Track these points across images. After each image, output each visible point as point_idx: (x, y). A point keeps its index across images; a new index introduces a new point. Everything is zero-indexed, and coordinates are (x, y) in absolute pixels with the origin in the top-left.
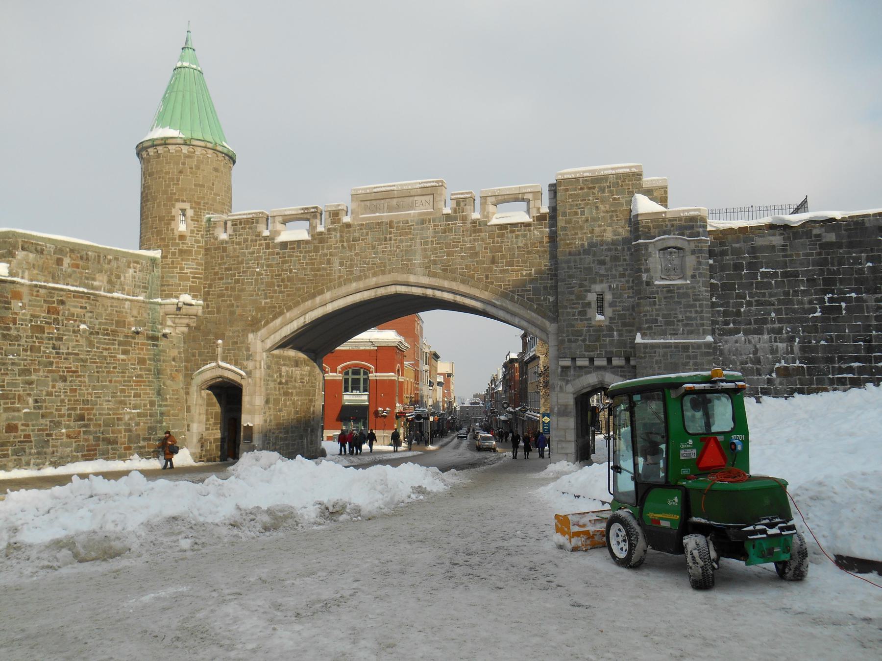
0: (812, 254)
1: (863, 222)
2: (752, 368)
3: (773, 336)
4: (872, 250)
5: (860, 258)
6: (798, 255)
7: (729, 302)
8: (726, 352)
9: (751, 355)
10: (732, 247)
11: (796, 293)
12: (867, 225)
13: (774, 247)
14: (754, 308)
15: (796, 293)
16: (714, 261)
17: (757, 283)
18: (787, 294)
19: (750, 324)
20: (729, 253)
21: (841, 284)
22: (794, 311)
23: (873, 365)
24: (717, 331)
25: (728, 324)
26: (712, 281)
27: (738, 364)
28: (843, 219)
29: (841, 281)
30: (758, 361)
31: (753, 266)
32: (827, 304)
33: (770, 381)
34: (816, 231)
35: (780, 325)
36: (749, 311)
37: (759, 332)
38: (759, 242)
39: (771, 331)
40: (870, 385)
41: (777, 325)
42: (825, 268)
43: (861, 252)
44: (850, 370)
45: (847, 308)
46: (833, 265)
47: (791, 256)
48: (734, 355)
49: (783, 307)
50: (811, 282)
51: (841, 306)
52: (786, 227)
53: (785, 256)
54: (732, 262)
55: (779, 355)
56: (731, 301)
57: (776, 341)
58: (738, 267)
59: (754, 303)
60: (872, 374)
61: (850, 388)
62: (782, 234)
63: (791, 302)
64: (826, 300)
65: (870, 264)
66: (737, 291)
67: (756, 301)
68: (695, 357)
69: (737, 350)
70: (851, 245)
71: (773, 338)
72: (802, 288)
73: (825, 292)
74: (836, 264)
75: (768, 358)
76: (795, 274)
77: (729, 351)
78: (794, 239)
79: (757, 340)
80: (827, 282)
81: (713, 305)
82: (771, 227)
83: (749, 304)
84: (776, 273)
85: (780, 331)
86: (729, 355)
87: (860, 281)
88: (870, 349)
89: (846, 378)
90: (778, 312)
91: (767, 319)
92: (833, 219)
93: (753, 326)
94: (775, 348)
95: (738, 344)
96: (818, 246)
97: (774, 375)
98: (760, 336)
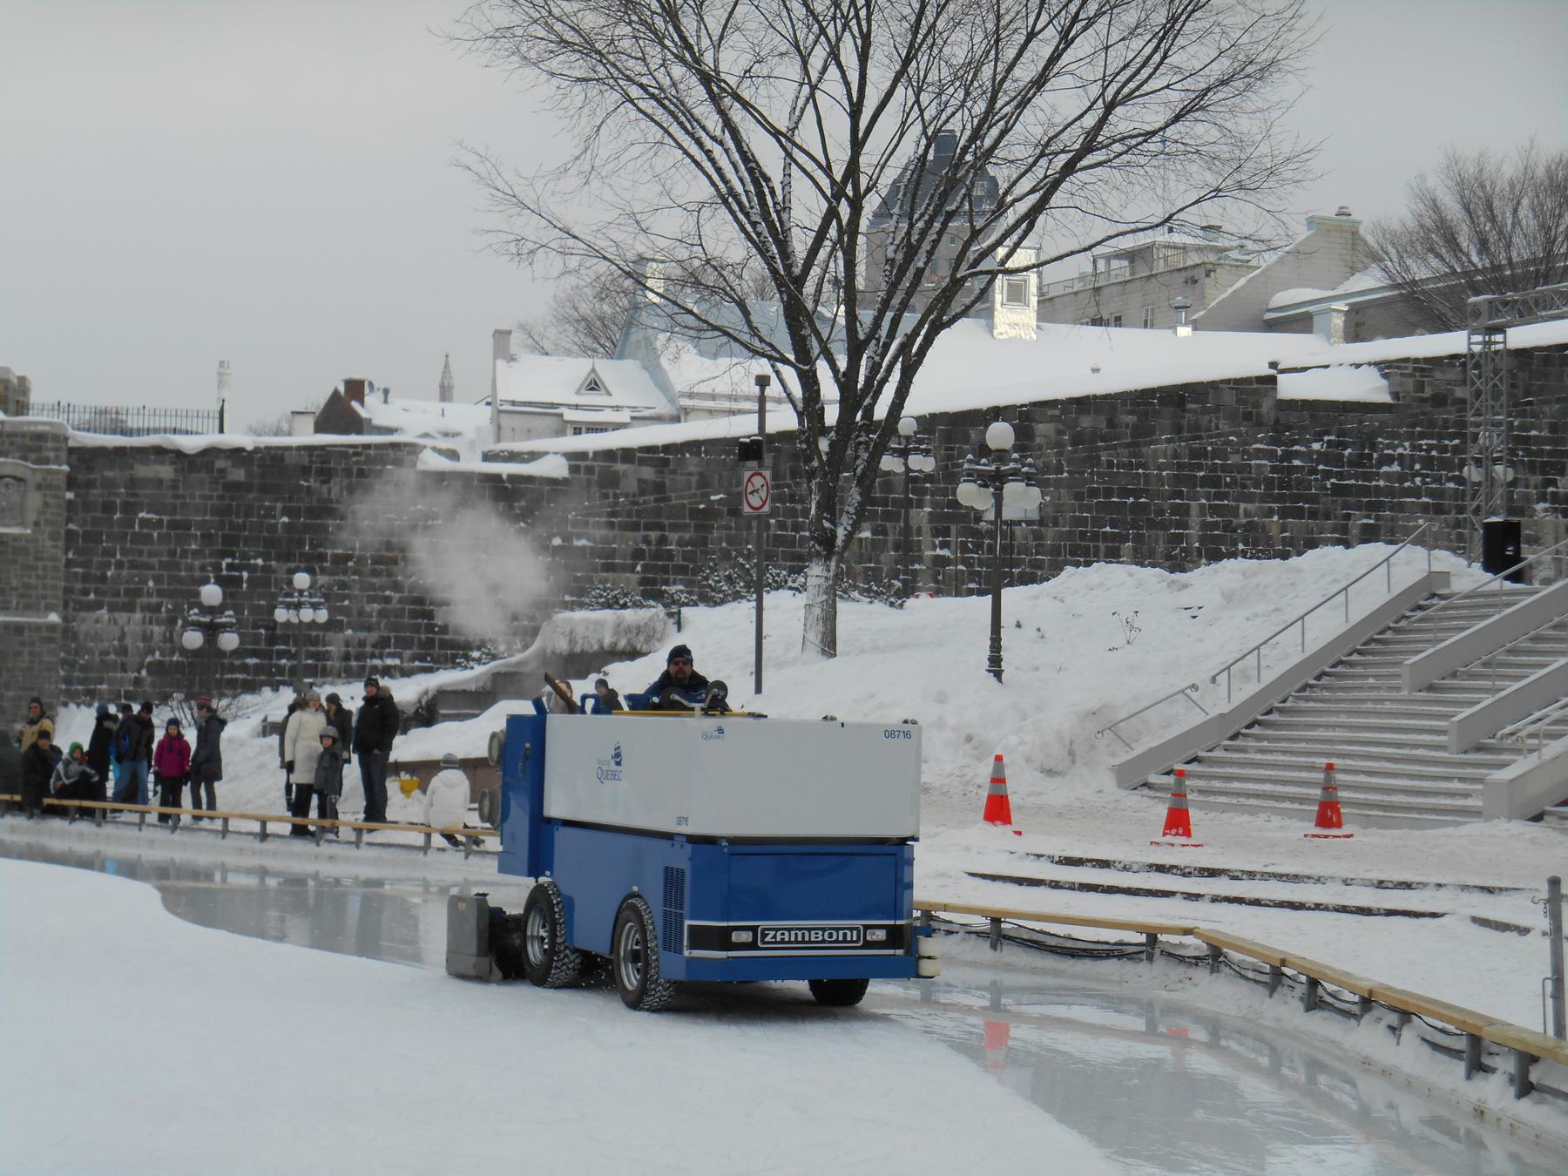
0: (211, 497)
1: (282, 458)
2: (116, 661)
3: (148, 615)
4: (290, 499)
5: (274, 508)
6: (193, 496)
7: (91, 561)
8: (81, 637)
9: (116, 643)
10: (102, 476)
11: (184, 553)
12: (287, 461)
13: (159, 482)
14: (125, 572)
15: (184, 553)
16: (76, 495)
17: (134, 534)
18: (172, 553)
19: (119, 595)
20: (98, 483)
21: (245, 544)
22: (180, 580)
23: (274, 662)
24: (71, 604)
25: (86, 593)
26: (72, 526)
27: (97, 654)
28: (257, 450)
29: (247, 541)
30: (123, 651)
31: (130, 508)
32: (225, 573)
33: (138, 682)
34: (220, 464)
35: (159, 600)
36: (119, 575)
37: (130, 608)
38: (143, 471)
39: (147, 608)
40: (267, 691)
41: (154, 600)
42: (227, 520)
43: (276, 501)
44: (245, 668)
45: (250, 580)
46: (238, 516)
47: (184, 497)
48: (92, 641)
49: (165, 573)
50: (207, 538)
51: (241, 577)
52: (179, 454)
53: (175, 497)
54: (100, 500)
55: (153, 644)
56: (95, 559)
57: (151, 623)
58: (108, 508)
59: (126, 565)
60: (272, 675)
61: (240, 694)
62: (172, 463)
63: (176, 566)
64: (224, 566)
65: (285, 519)
66: (104, 544)
67: (129, 561)
68: (32, 644)
69: (97, 633)
70: (264, 489)
71: (147, 618)
72: (194, 547)
73: (224, 555)
74: (242, 514)
75: (138, 647)
76: (186, 525)
77: (86, 635)
78: (191, 471)
79: (125, 619)
80: (230, 541)
81: (69, 563)
82: (159, 452)
83: (119, 565)
84: (160, 522)
85: (157, 609)
86: (86, 640)
87: (270, 543)
88: (272, 640)
89: (236, 680)
90: (158, 580)
91: (142, 589)
92: (240, 450)
93: (123, 599)
94: (148, 632)
95: (99, 625)
96: (220, 487)
97: (144, 673)
98: (130, 615)
